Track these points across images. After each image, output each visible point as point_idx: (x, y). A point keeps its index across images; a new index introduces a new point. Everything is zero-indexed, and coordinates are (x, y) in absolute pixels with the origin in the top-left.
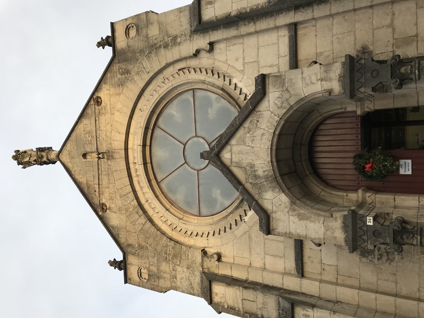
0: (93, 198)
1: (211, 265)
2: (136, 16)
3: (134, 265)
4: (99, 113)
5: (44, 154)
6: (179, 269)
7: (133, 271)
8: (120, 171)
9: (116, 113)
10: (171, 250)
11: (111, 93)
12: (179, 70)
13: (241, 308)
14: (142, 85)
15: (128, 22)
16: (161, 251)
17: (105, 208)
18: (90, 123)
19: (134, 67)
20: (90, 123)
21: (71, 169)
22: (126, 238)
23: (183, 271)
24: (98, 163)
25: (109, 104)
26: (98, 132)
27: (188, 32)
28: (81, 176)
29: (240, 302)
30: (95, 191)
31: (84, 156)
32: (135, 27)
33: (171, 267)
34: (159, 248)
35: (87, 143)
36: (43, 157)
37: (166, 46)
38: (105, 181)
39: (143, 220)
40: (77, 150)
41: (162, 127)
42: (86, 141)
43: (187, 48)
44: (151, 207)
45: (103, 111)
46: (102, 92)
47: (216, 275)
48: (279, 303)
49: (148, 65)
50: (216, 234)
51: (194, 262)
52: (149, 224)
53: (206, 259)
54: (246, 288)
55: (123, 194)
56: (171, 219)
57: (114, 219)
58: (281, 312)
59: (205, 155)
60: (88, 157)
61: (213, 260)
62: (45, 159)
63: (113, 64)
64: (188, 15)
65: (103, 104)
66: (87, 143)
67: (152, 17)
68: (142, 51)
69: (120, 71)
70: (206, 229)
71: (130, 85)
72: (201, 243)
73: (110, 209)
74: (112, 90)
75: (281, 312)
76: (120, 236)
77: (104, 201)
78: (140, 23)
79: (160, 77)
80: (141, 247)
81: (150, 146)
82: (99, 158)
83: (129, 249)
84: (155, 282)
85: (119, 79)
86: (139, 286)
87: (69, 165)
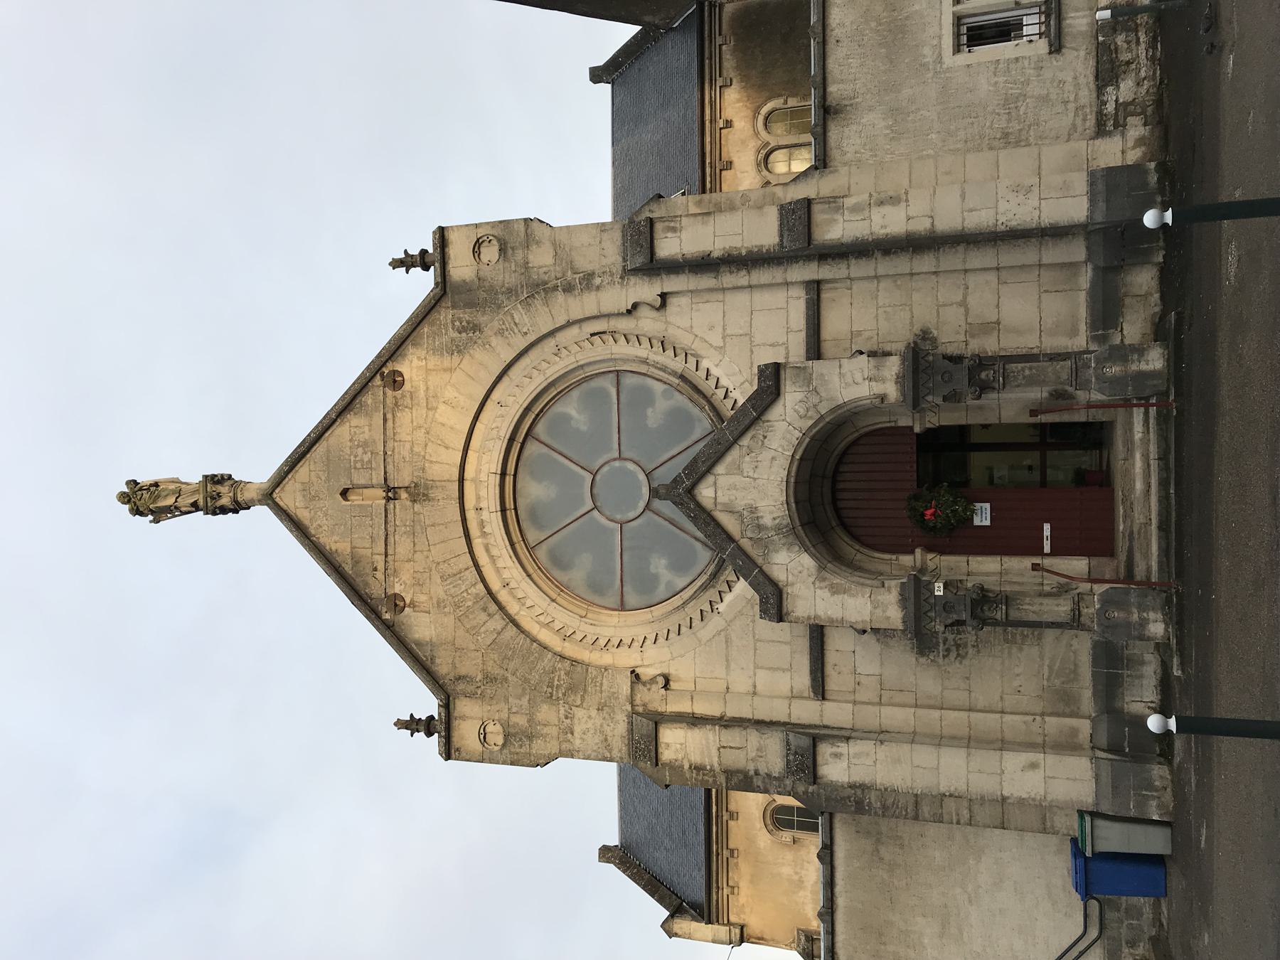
0: (367, 584)
1: (653, 698)
2: (501, 222)
3: (471, 718)
4: (396, 404)
5: (223, 489)
6: (579, 713)
7: (466, 733)
8: (446, 525)
9: (442, 407)
10: (563, 676)
11: (431, 366)
12: (592, 335)
13: (716, 765)
14: (509, 356)
15: (481, 232)
16: (541, 681)
17: (402, 604)
18: (370, 425)
19: (492, 320)
20: (370, 425)
21: (307, 522)
22: (453, 663)
23: (590, 717)
24: (386, 510)
25: (422, 388)
26: (390, 444)
27: (618, 269)
28: (336, 538)
29: (714, 753)
30: (375, 569)
31: (344, 493)
32: (495, 242)
33: (562, 711)
34: (534, 678)
35: (359, 465)
36: (219, 496)
37: (569, 289)
38: (402, 546)
39: (497, 622)
40: (328, 480)
41: (543, 437)
42: (356, 462)
43: (616, 297)
44: (514, 597)
45: (408, 401)
46: (407, 362)
47: (661, 714)
48: (788, 744)
49: (527, 320)
50: (661, 640)
51: (614, 696)
52: (512, 630)
53: (641, 687)
54: (726, 727)
55: (450, 571)
56: (563, 617)
57: (421, 627)
58: (791, 757)
59: (662, 491)
60: (351, 497)
61: (654, 688)
62: (225, 501)
63: (437, 308)
64: (620, 239)
65: (407, 386)
66: (359, 465)
67: (537, 230)
68: (511, 292)
69: (457, 323)
70: (640, 632)
71: (478, 353)
72: (627, 658)
73: (413, 605)
74: (433, 361)
75: (791, 757)
76: (438, 661)
77: (398, 589)
78: (511, 238)
79: (550, 344)
80: (489, 679)
81: (515, 476)
82: (388, 499)
83: (461, 687)
84: (521, 746)
85: (453, 340)
86: (482, 760)
87: (303, 515)
